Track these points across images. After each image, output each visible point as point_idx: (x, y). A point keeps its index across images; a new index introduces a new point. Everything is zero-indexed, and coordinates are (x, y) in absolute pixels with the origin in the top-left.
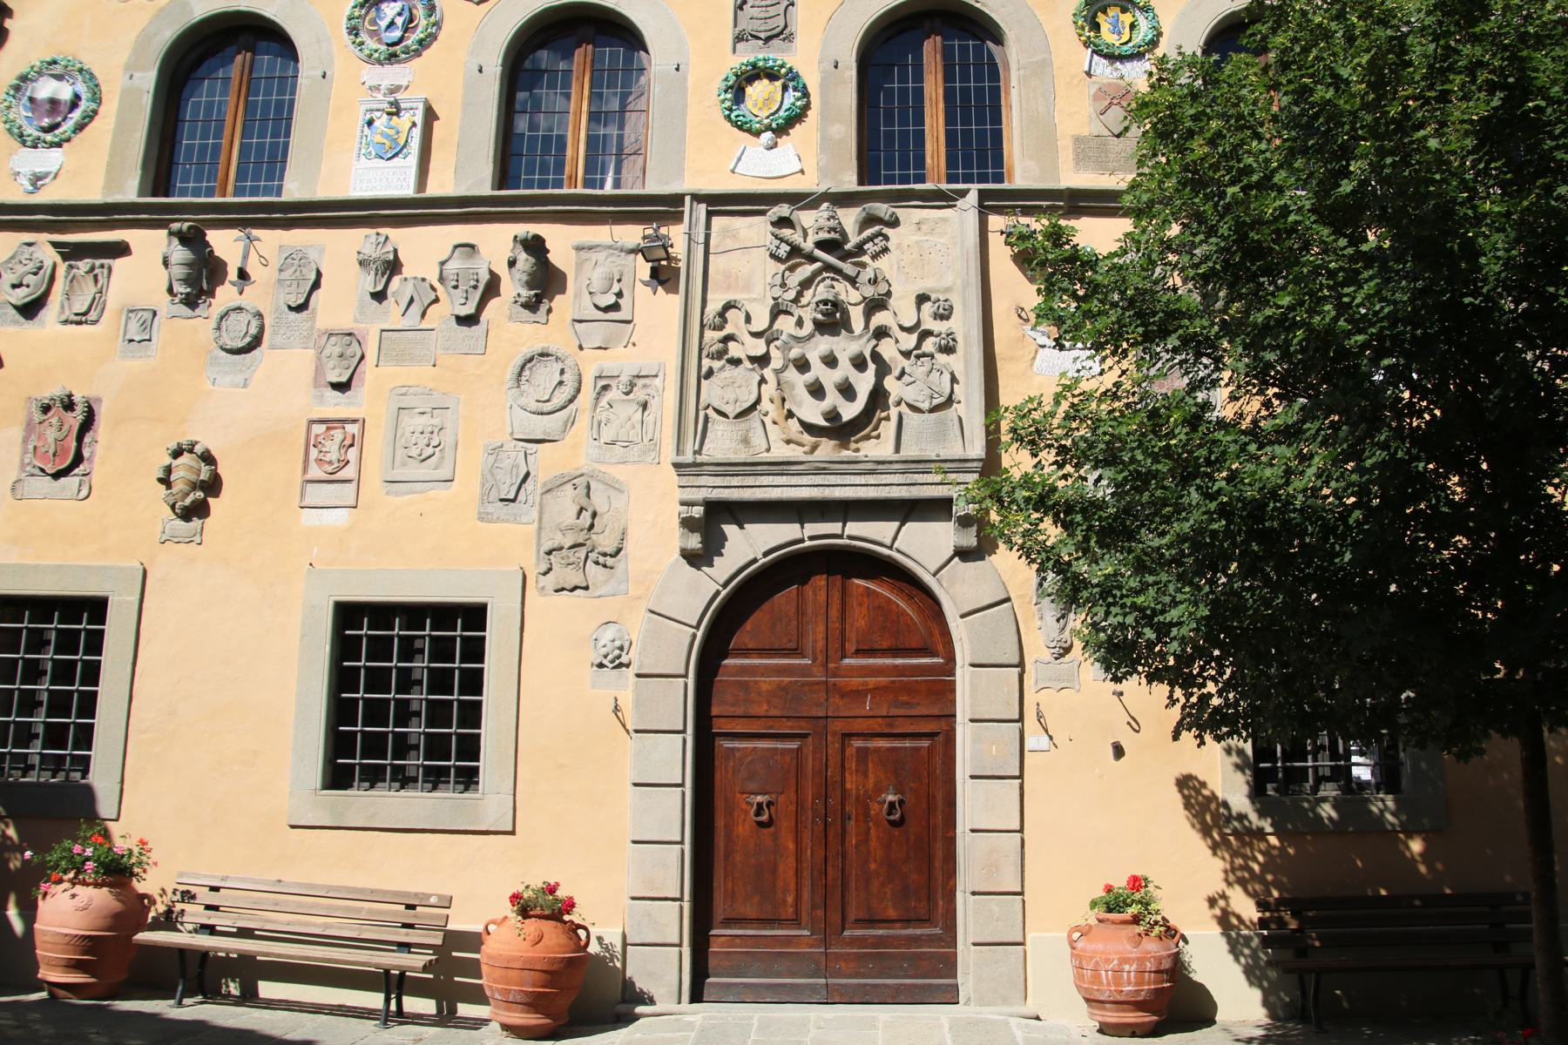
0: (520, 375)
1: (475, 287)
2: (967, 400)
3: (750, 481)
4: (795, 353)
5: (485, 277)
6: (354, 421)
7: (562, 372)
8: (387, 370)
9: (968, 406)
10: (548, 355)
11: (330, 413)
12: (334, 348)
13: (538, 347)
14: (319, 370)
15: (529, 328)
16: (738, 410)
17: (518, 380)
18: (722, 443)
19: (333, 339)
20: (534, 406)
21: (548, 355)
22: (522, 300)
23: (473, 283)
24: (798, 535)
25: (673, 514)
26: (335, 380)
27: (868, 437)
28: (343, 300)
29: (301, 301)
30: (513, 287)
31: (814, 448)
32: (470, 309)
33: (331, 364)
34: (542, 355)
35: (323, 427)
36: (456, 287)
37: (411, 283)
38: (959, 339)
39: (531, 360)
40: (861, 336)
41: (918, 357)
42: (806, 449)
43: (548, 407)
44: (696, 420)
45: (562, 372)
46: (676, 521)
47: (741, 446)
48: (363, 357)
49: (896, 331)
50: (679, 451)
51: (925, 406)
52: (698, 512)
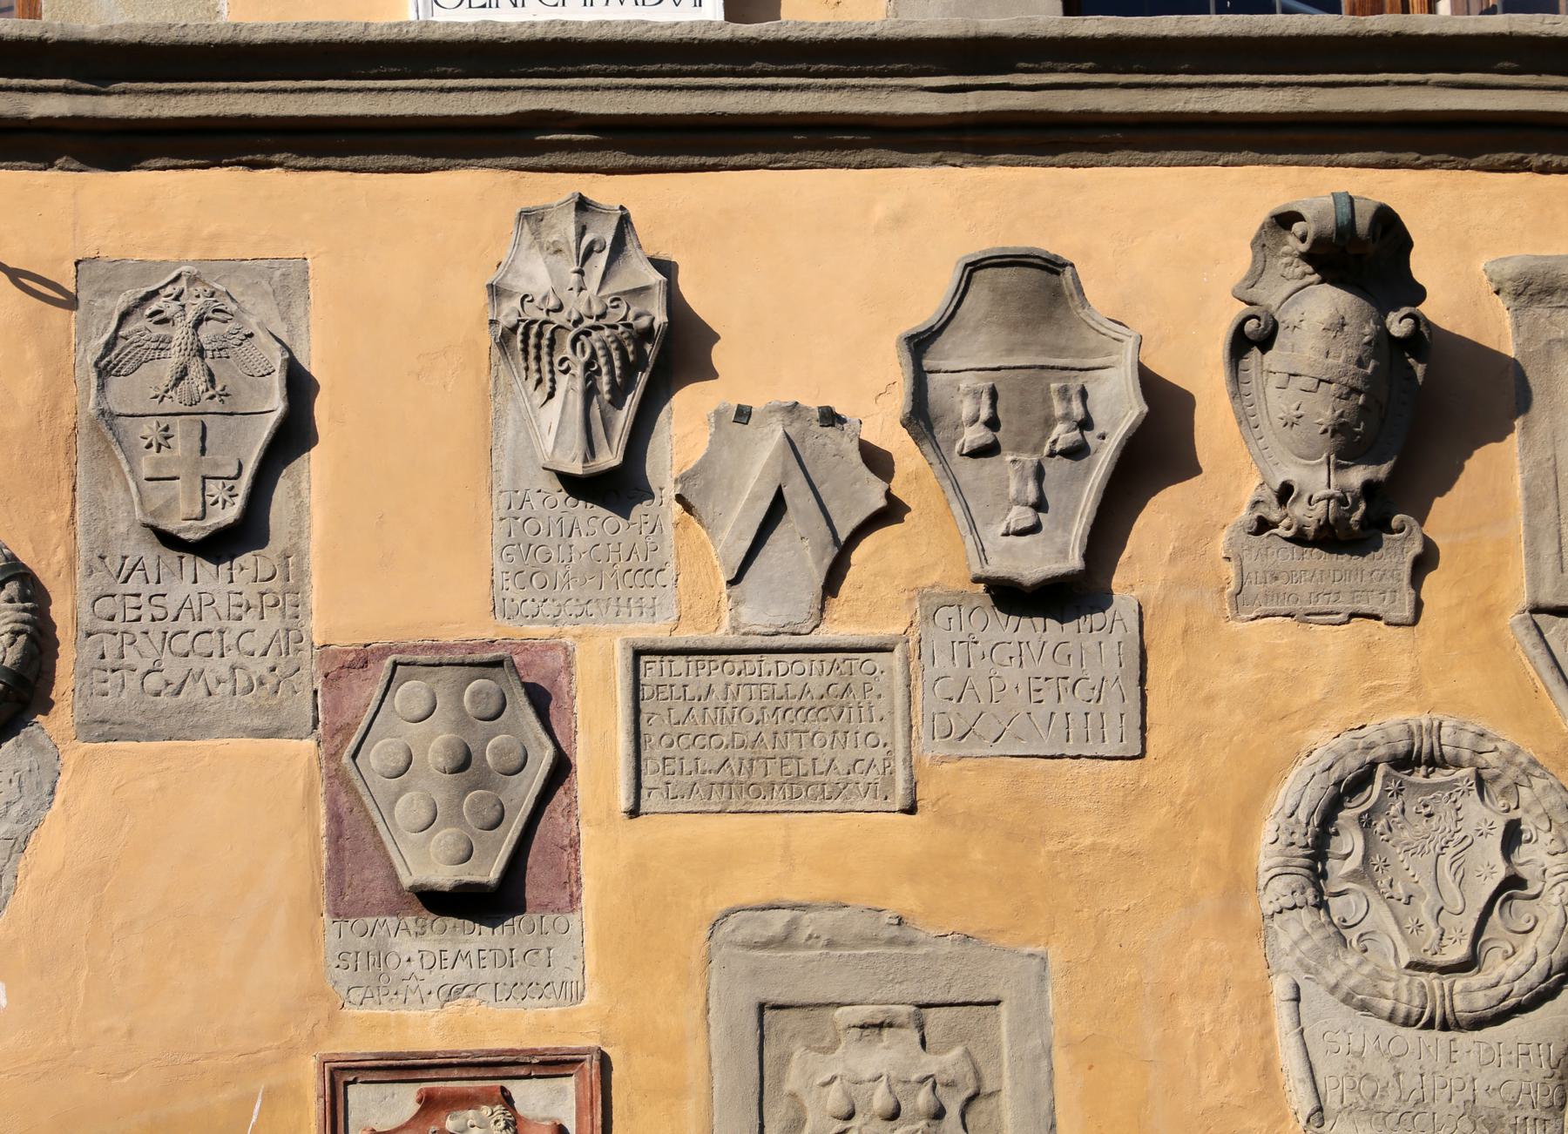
0: (1320, 849)
1: (1077, 452)
5: (1119, 409)
6: (554, 1065)
7: (1512, 837)
8: (674, 832)
10: (1435, 762)
11: (427, 1029)
12: (414, 730)
13: (1390, 725)
14: (350, 839)
15: (1335, 642)
17: (1317, 876)
19: (411, 693)
20: (1405, 991)
21: (1435, 762)
22: (1308, 514)
23: (1063, 435)
26: (444, 876)
28: (419, 515)
29: (229, 514)
30: (1262, 447)
32: (1057, 553)
33: (409, 808)
34: (1404, 762)
35: (404, 1100)
36: (988, 451)
37: (766, 443)
39: (1363, 780)
43: (1471, 993)
45: (1512, 837)
48: (561, 769)
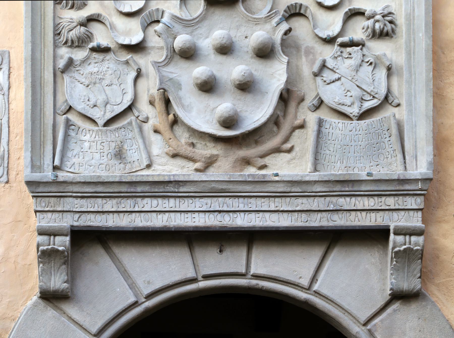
2: (410, 104)
3: (127, 204)
4: (181, 40)
9: (410, 111)
16: (109, 115)
18: (89, 158)
24: (191, 274)
25: (28, 246)
27: (278, 150)
31: (210, 163)
38: (401, 20)
40: (269, 17)
41: (344, 45)
42: (198, 165)
44: (53, 124)
46: (33, 255)
47: (114, 162)
49: (313, 9)
50: (35, 166)
51: (355, 111)
52: (62, 243)
